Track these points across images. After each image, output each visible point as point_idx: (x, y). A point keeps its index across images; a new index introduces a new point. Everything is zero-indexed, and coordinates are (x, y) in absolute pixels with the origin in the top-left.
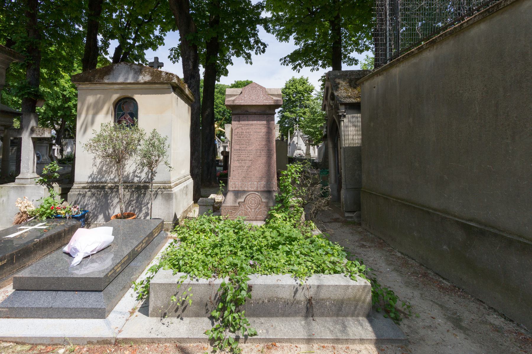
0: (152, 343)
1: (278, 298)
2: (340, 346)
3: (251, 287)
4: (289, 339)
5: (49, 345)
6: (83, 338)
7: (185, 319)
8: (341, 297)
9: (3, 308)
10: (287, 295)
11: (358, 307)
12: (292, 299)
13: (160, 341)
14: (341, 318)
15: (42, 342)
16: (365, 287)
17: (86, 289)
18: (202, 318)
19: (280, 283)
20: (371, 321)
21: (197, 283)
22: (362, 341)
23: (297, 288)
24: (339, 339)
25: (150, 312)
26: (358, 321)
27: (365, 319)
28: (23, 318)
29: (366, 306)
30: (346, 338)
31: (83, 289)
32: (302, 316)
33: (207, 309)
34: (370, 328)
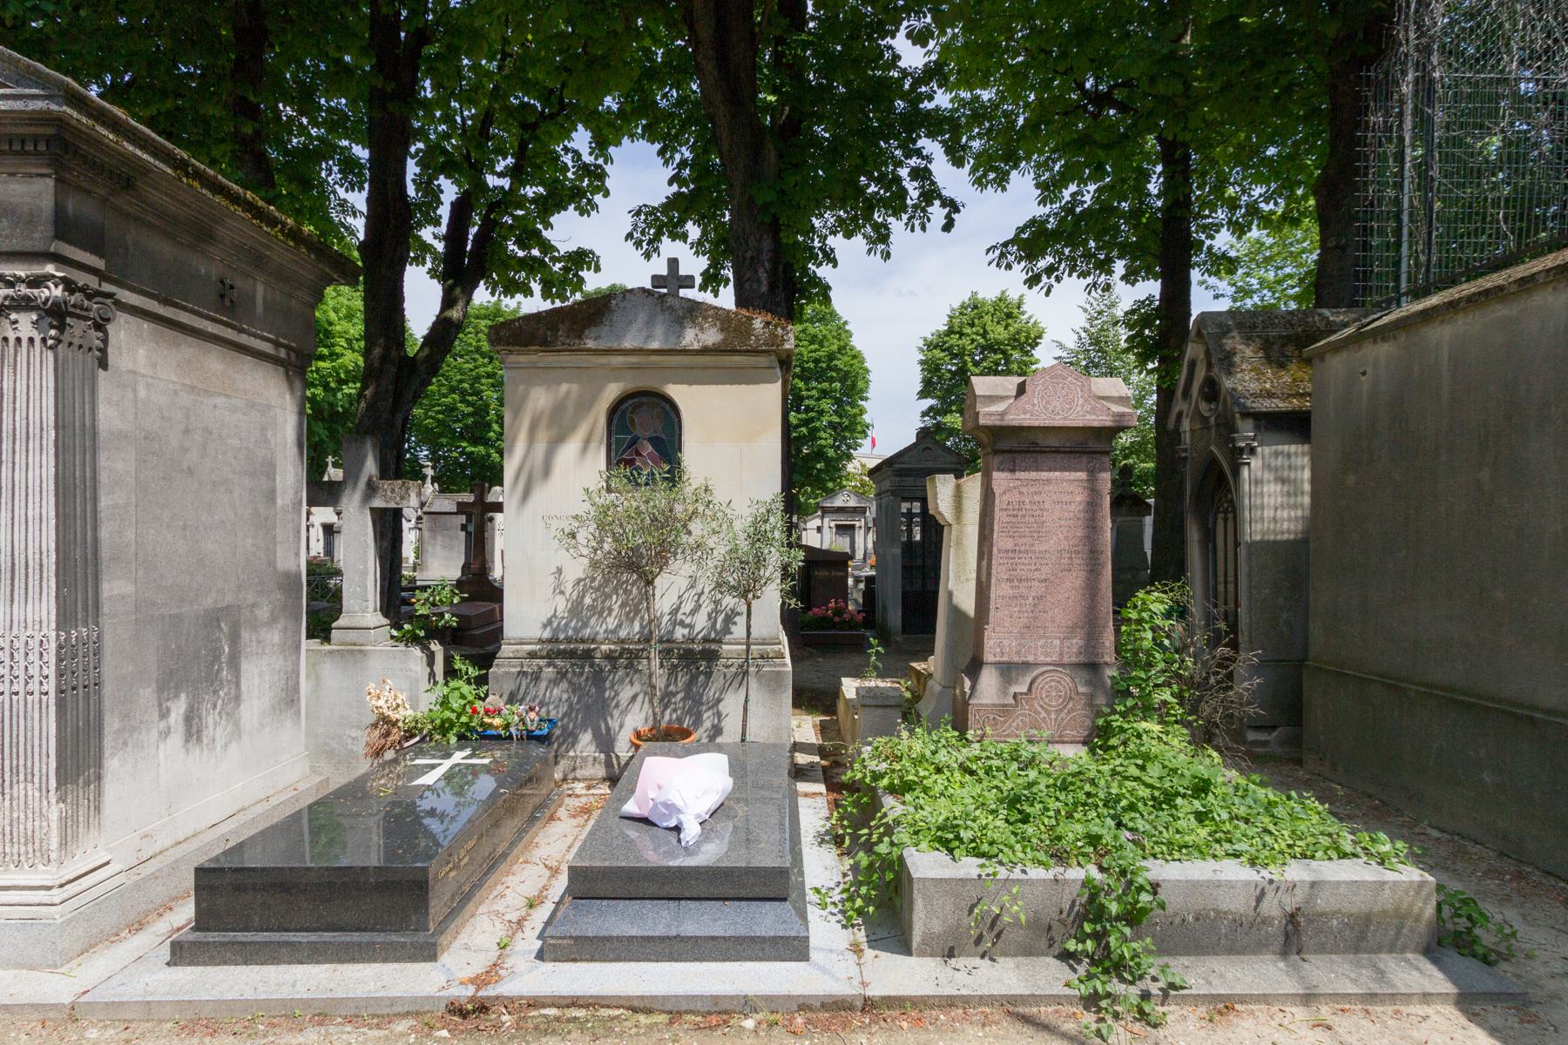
0: (950, 1006)
1: (1217, 912)
2: (1378, 1009)
3: (1158, 885)
4: (1264, 995)
5: (710, 1013)
6: (789, 997)
7: (1001, 960)
8: (1364, 909)
9: (560, 938)
10: (1239, 904)
11: (1405, 931)
12: (1251, 913)
13: (968, 1003)
14: (1366, 956)
15: (692, 1007)
16: (1422, 884)
17: (750, 896)
18: (1041, 959)
19: (1222, 877)
20: (1435, 961)
21: (1024, 876)
22: (1426, 998)
23: (1263, 889)
24: (1376, 994)
25: (915, 945)
26: (1407, 961)
27: (1421, 958)
28: (610, 961)
29: (1422, 927)
30: (1390, 991)
31: (743, 894)
32: (1274, 953)
33: (1052, 939)
34: (1440, 975)
